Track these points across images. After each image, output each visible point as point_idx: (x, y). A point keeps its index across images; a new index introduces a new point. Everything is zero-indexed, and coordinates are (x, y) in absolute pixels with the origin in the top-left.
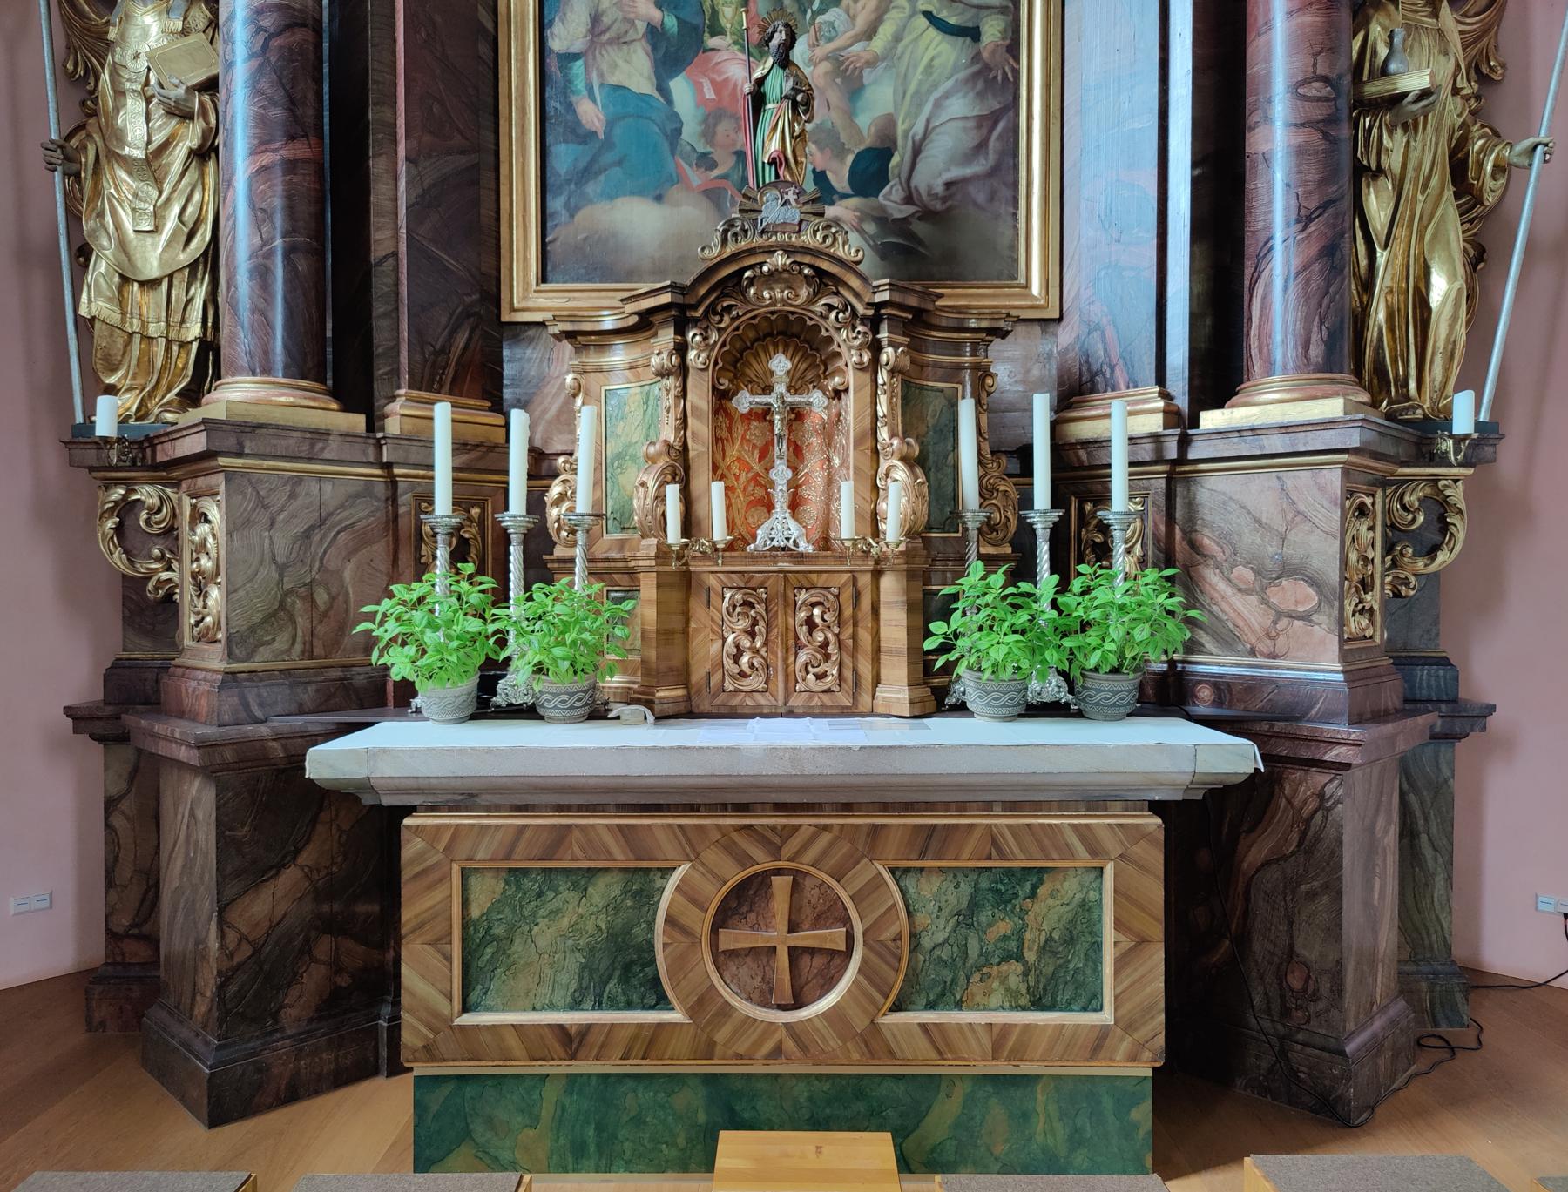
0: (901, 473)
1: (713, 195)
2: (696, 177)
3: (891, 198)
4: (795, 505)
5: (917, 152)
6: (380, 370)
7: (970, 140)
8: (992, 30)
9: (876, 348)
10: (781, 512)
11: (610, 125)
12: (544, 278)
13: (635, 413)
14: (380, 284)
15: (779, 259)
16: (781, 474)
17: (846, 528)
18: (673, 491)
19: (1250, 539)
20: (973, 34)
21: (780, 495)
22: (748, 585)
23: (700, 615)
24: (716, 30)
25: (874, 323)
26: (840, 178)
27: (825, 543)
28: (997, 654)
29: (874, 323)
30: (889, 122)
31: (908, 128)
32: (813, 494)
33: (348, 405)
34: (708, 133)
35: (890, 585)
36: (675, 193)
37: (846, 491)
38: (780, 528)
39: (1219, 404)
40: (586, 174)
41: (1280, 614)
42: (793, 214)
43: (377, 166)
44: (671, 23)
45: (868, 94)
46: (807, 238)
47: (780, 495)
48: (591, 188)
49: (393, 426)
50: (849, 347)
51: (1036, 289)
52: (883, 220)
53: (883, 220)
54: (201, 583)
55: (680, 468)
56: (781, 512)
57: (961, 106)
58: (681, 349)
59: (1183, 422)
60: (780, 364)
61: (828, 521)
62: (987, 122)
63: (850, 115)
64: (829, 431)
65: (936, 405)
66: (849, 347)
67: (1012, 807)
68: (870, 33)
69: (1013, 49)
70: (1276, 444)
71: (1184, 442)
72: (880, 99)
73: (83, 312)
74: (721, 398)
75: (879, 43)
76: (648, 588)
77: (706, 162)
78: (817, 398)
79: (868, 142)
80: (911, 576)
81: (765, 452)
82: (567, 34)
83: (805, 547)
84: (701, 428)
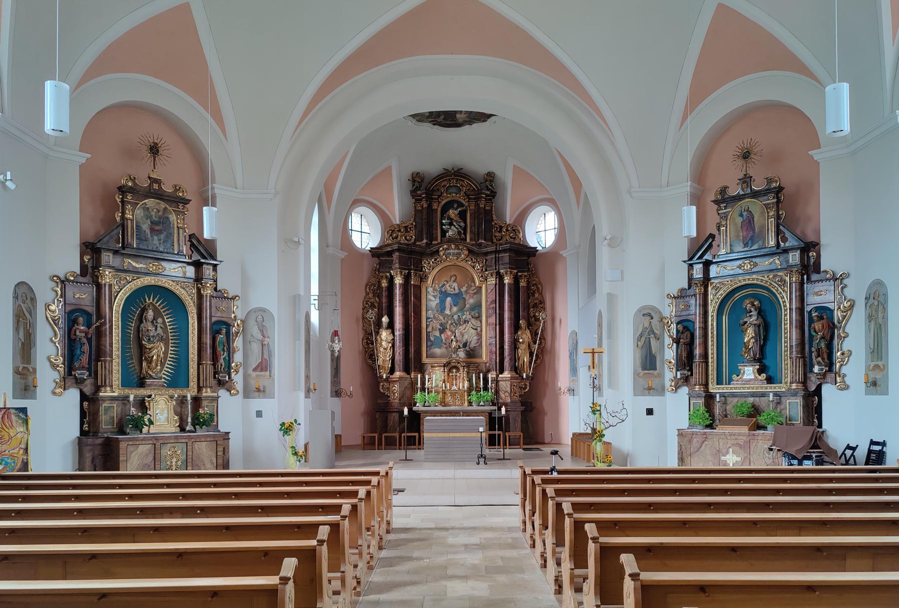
0: (467, 382)
1: (446, 348)
2: (444, 346)
3: (467, 348)
4: (456, 385)
5: (470, 343)
6: (411, 370)
7: (477, 341)
8: (479, 329)
9: (464, 369)
10: (454, 386)
11: (434, 340)
12: (427, 358)
13: (438, 375)
14: (410, 361)
15: (454, 361)
16: (454, 382)
17: (461, 388)
18: (444, 384)
19: (504, 389)
20: (477, 329)
21: (454, 384)
22: (451, 393)
23: (446, 396)
24: (447, 329)
25: (464, 367)
26: (461, 346)
27: (459, 389)
28: (474, 399)
29: (464, 367)
30: (467, 339)
31: (469, 340)
32: (458, 384)
33: (408, 375)
34: (446, 341)
35: (465, 393)
36: (442, 348)
37: (461, 384)
38: (454, 388)
39: (502, 374)
40: (432, 345)
41: (506, 396)
42: (456, 356)
43: (410, 348)
44: (442, 328)
45: (465, 336)
46: (457, 359)
47: (454, 384)
48: (432, 347)
49: (412, 377)
50: (461, 369)
51: (484, 359)
52: (466, 351)
53: (466, 351)
54: (394, 394)
55: (444, 381)
56: (454, 386)
57: (475, 338)
58: (444, 369)
59: (497, 376)
60: (454, 370)
61: (459, 386)
62: (478, 339)
63: (462, 339)
64: (460, 377)
65: (471, 374)
66: (461, 369)
67: (475, 413)
68: (465, 329)
69: (481, 331)
70: (504, 379)
71: (497, 378)
72: (466, 337)
73: (379, 364)
74: (448, 374)
75: (466, 331)
76: (441, 394)
77: (446, 344)
78: (458, 374)
79: (465, 342)
80: (468, 392)
81: (453, 379)
82: (430, 329)
83: (457, 389)
84: (446, 377)
